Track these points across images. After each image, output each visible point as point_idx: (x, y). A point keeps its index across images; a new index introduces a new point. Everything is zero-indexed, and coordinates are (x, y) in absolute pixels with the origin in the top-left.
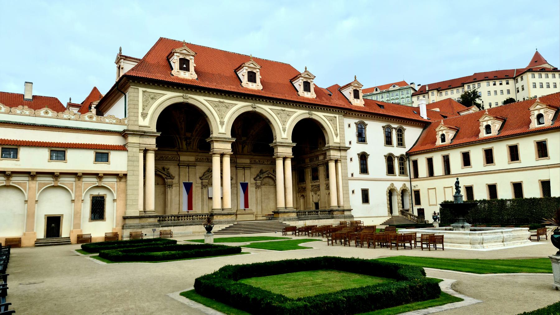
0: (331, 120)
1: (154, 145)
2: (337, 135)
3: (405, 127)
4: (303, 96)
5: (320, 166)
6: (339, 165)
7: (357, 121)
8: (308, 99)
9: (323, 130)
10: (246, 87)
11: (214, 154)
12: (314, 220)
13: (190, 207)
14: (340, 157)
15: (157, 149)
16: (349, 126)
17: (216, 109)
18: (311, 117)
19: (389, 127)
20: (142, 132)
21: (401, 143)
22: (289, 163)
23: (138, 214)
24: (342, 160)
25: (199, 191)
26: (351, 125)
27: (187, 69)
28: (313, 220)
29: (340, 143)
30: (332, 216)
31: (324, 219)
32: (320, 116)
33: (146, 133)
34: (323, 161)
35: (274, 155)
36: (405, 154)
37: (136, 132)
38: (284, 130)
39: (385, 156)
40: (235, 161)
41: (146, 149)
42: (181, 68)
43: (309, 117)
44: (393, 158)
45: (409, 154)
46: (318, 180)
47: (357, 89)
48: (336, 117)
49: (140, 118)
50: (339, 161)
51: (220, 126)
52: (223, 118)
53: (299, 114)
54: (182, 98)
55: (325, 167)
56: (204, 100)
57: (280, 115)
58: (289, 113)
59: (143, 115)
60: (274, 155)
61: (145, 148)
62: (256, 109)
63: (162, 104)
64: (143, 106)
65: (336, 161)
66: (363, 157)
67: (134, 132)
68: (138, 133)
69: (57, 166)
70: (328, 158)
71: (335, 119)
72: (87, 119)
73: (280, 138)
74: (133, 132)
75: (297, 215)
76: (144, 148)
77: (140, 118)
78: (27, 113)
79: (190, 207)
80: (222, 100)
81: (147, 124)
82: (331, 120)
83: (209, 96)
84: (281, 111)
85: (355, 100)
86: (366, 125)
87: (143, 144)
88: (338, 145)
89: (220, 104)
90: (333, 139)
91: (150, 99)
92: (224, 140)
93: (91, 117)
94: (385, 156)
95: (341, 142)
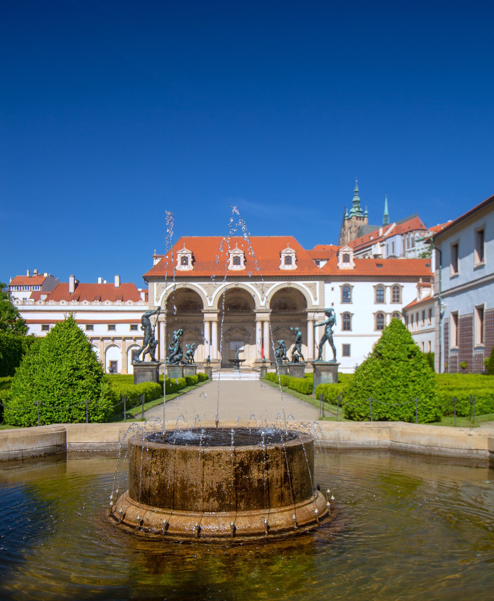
0: (310, 286)
2: (316, 299)
3: (401, 284)
7: (342, 284)
8: (288, 271)
16: (333, 289)
17: (206, 289)
18: (289, 286)
19: (380, 286)
21: (396, 299)
22: (266, 325)
26: (335, 289)
27: (186, 264)
32: (300, 285)
36: (400, 310)
38: (263, 300)
39: (374, 314)
42: (182, 264)
44: (384, 315)
45: (405, 310)
49: (155, 302)
53: (277, 285)
64: (157, 293)
65: (314, 321)
66: (347, 316)
69: (112, 334)
71: (314, 285)
72: (128, 304)
75: (271, 365)
77: (155, 302)
78: (99, 304)
82: (311, 287)
85: (344, 264)
86: (353, 287)
88: (315, 308)
90: (313, 303)
91: (161, 288)
93: (130, 303)
94: (374, 314)
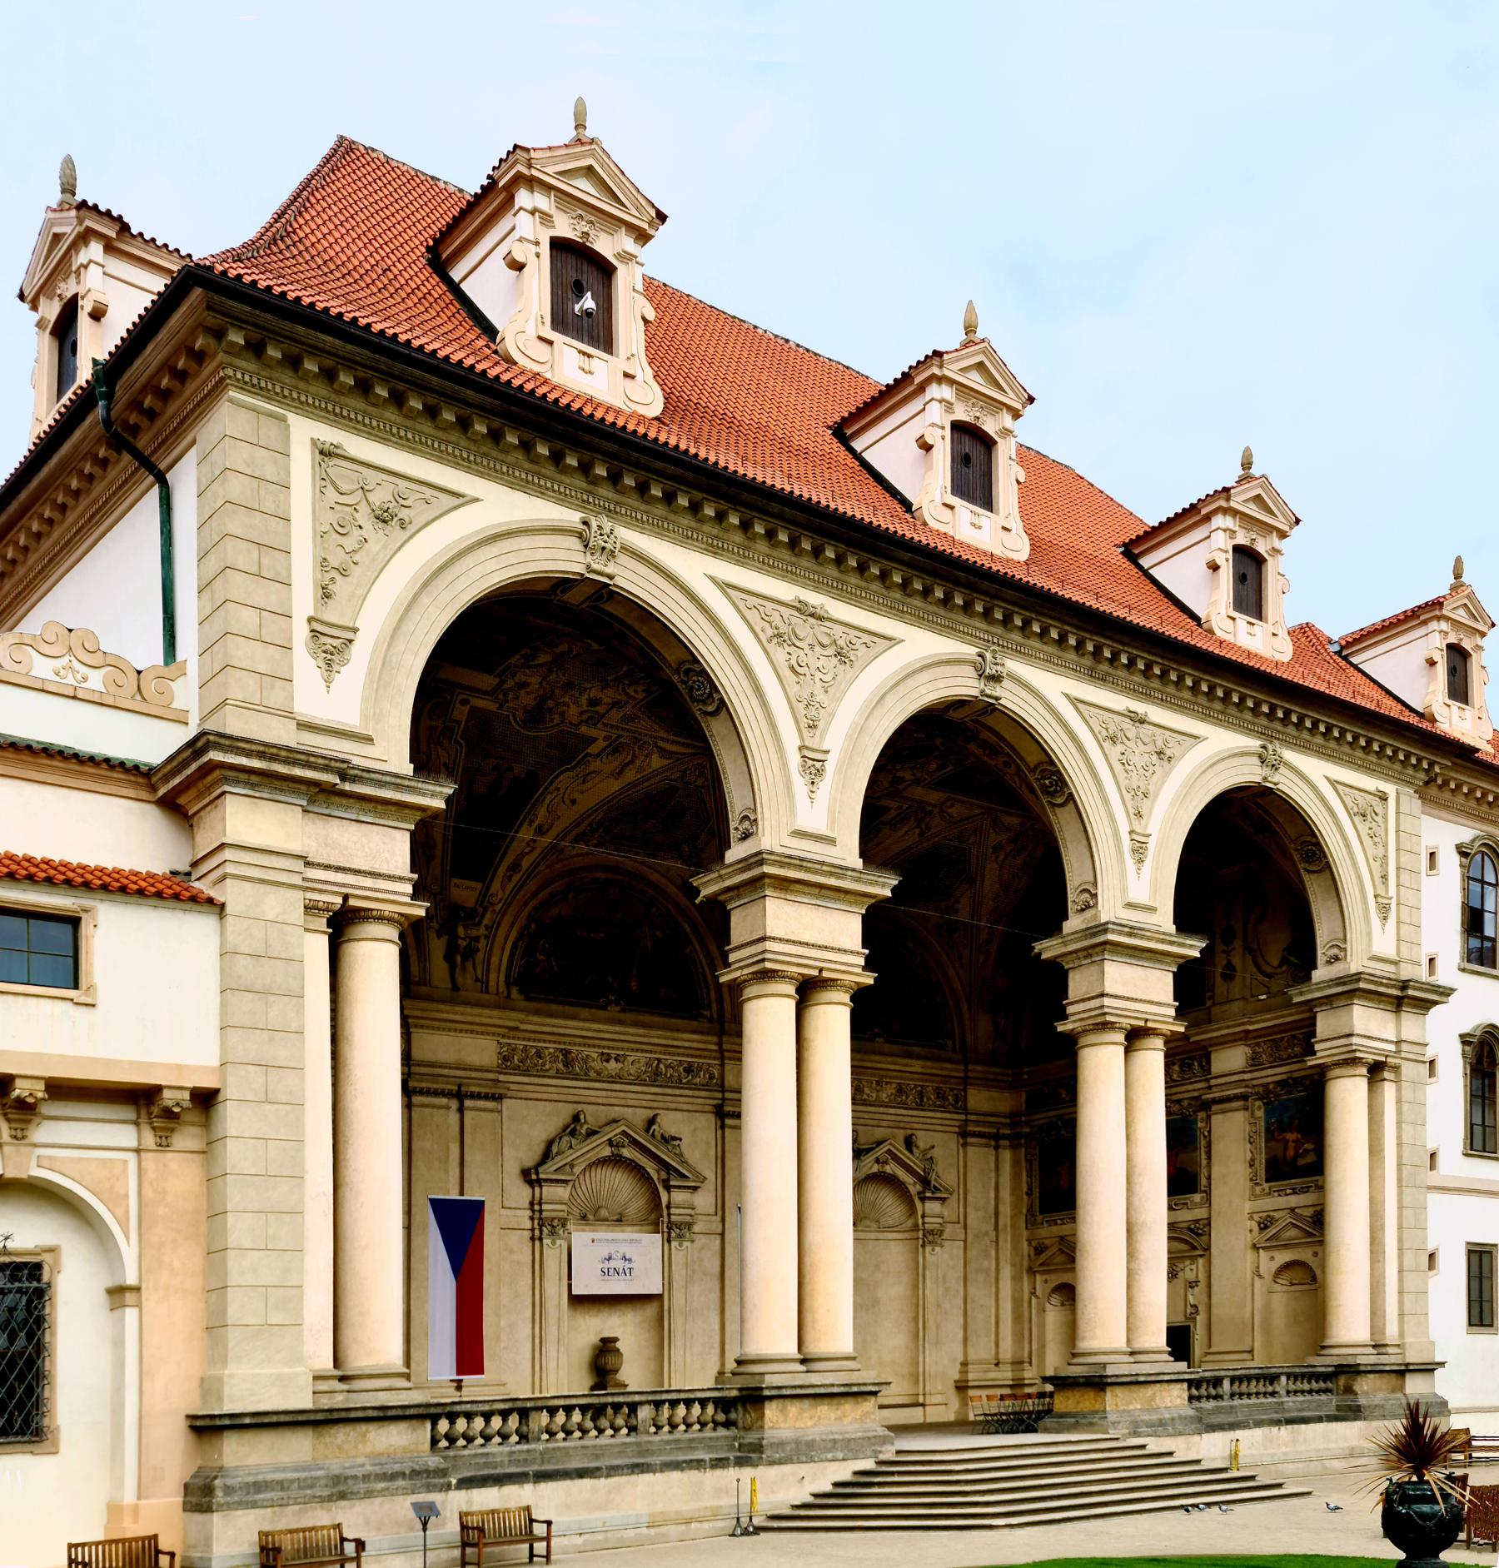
1: (401, 879)
4: (1228, 638)
5: (1215, 1108)
6: (1389, 1090)
9: (1306, 877)
10: (942, 528)
11: (767, 975)
12: (1275, 1429)
13: (470, 1357)
14: (1392, 1047)
15: (422, 913)
20: (326, 769)
23: (301, 1399)
24: (1405, 1066)
25: (515, 1257)
28: (1266, 1430)
29: (1395, 963)
30: (1348, 1400)
31: (1320, 1420)
33: (354, 779)
34: (1246, 1076)
35: (1065, 1017)
37: (287, 762)
40: (712, 1077)
41: (352, 902)
43: (1258, 779)
46: (1197, 1197)
47: (1463, 644)
48: (1384, 798)
50: (1386, 1075)
51: (800, 784)
52: (821, 725)
54: (575, 543)
55: (1260, 1113)
56: (712, 578)
57: (1120, 748)
58: (1166, 742)
59: (324, 639)
60: (1065, 1017)
61: (346, 897)
62: (997, 691)
63: (449, 575)
65: (1376, 1070)
67: (274, 758)
68: (298, 772)
70: (1324, 1052)
73: (1119, 905)
74: (261, 755)
76: (339, 900)
79: (470, 1357)
80: (814, 598)
81: (350, 719)
83: (742, 559)
84: (1126, 724)
87: (328, 867)
89: (805, 628)
92: (833, 882)
95: (1405, 954)
